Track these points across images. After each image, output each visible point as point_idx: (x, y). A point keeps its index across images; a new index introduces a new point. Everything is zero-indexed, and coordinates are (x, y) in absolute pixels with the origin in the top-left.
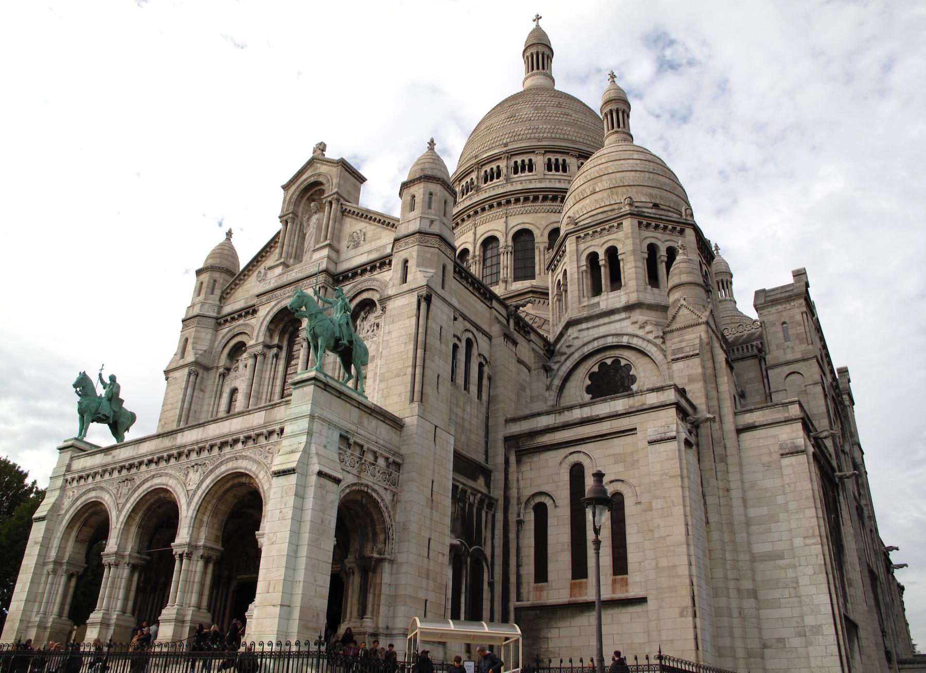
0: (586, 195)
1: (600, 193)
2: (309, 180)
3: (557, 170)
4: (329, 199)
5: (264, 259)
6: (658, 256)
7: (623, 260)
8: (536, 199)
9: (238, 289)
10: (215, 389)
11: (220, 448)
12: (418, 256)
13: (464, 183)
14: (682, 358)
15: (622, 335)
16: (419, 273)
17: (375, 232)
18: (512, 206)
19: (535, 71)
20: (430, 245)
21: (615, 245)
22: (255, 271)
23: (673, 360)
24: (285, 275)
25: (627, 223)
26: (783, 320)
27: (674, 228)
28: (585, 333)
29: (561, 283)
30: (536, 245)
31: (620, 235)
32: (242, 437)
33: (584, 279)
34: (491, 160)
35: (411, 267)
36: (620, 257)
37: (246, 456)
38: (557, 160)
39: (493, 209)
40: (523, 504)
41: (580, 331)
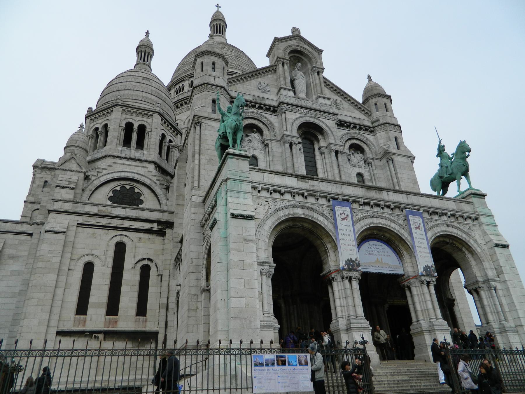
2: (296, 47)
9: (238, 84)
11: (431, 214)
19: (221, 34)
32: (449, 213)
37: (456, 227)
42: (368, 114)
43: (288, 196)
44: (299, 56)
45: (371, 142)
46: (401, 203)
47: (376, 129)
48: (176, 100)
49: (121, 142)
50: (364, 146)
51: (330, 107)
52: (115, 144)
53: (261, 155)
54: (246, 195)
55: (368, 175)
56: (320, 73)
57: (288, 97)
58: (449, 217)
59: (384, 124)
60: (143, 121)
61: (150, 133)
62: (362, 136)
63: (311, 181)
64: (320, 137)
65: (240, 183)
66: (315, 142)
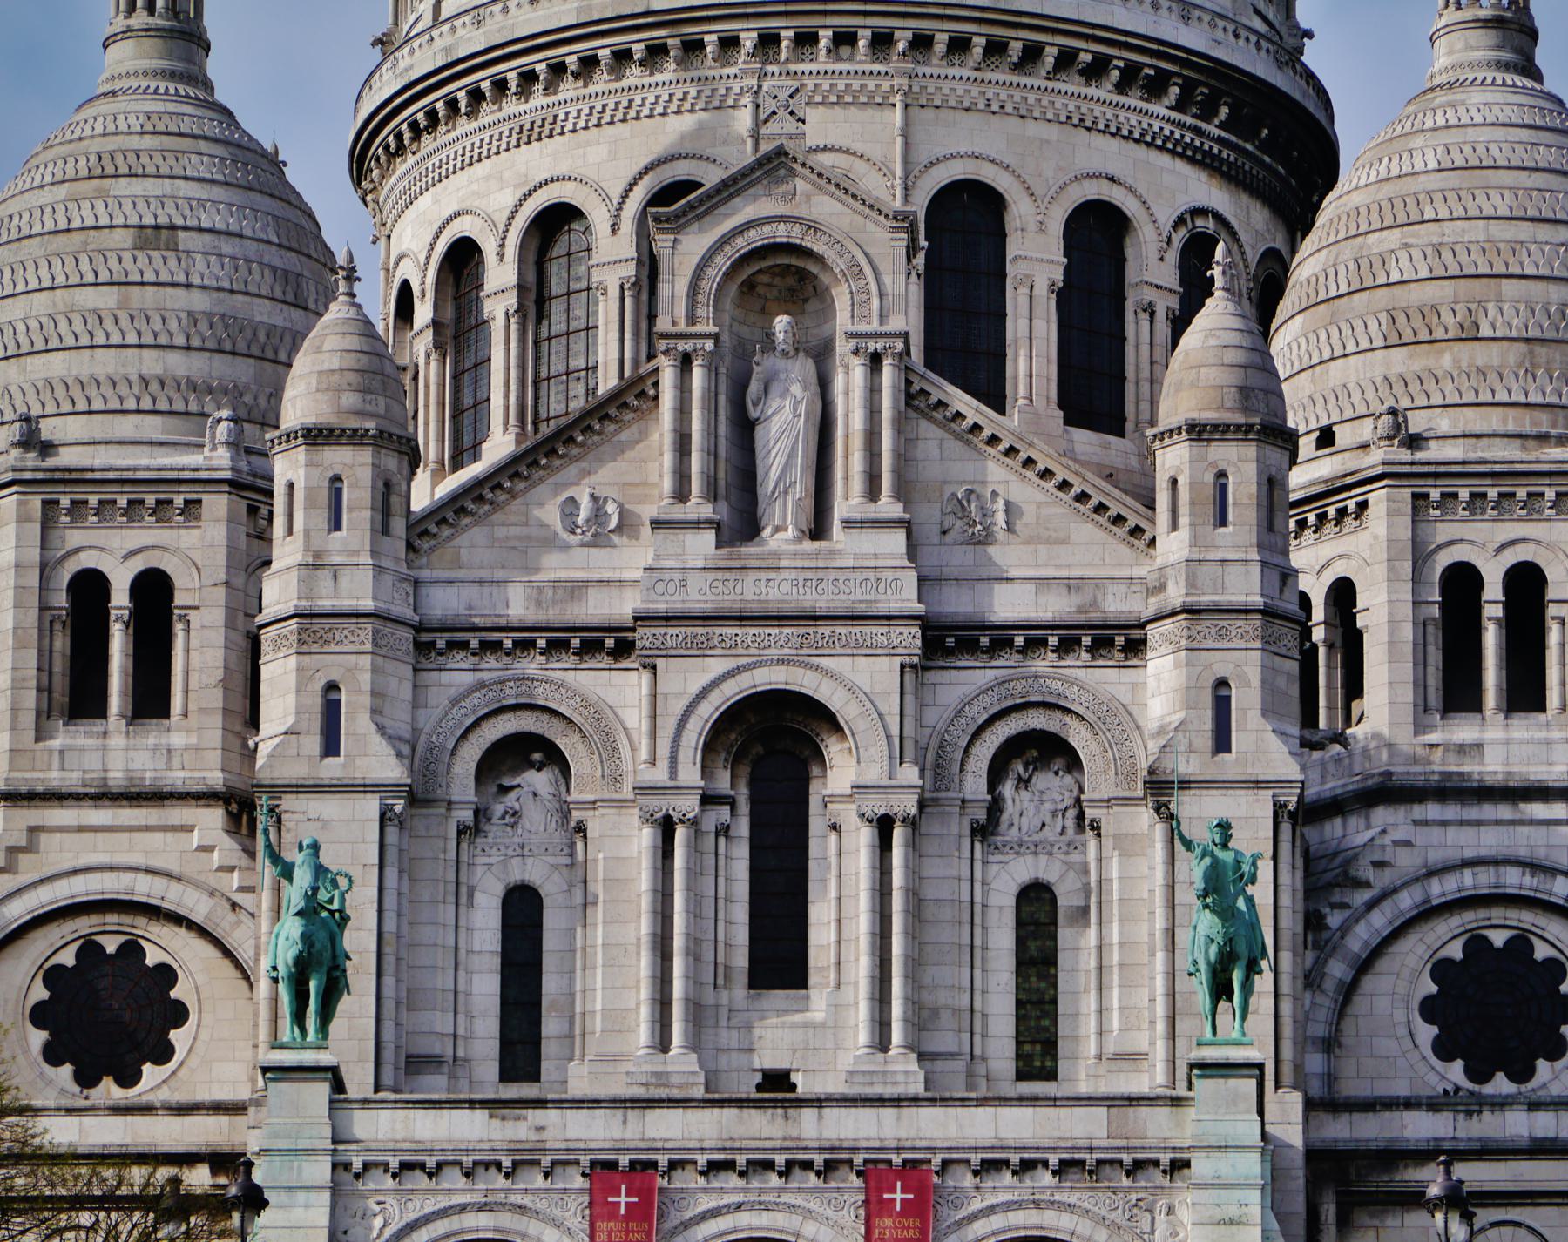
0: (1439, 334)
1: (1495, 346)
2: (767, 229)
4: (872, 346)
5: (575, 451)
8: (1032, 54)
10: (452, 876)
12: (1263, 681)
16: (1273, 737)
17: (1045, 511)
18: (936, 66)
20: (1283, 651)
21: (1542, 564)
22: (534, 485)
24: (752, 576)
28: (1436, 832)
29: (1318, 614)
32: (1053, 1160)
33: (1431, 649)
35: (1244, 711)
36: (1552, 610)
39: (845, 51)
41: (1416, 823)
43: (453, 1179)
44: (794, 261)
46: (855, 1149)
47: (1153, 631)
48: (440, 63)
49: (56, 695)
50: (1078, 737)
51: (889, 575)
52: (28, 719)
53: (556, 876)
54: (313, 1196)
55: (1079, 885)
57: (677, 576)
59: (1174, 614)
60: (154, 548)
61: (193, 616)
63: (539, 1113)
65: (296, 1161)
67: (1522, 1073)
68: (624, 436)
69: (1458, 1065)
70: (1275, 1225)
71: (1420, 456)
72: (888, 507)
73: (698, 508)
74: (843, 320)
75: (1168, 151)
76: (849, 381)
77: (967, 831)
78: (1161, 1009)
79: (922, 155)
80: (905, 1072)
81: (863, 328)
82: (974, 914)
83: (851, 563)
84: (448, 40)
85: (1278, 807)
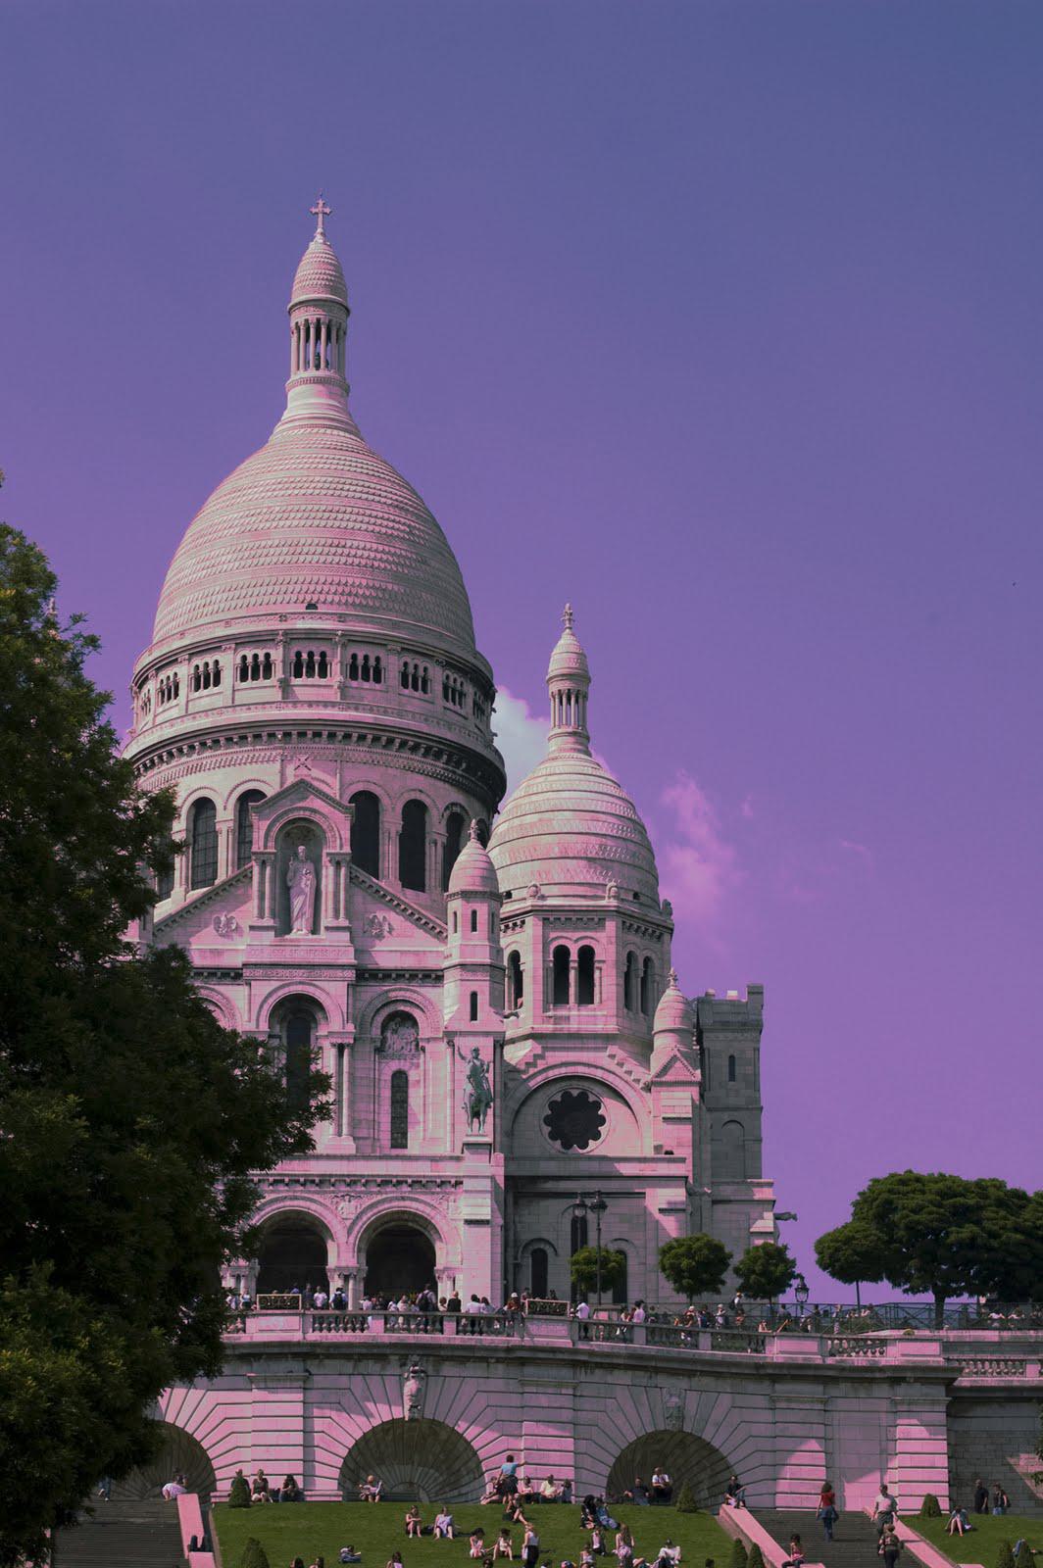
1: (575, 861)
3: (416, 689)
6: (633, 967)
7: (600, 969)
8: (390, 741)
13: (249, 653)
14: (674, 1118)
15: (596, 1067)
23: (664, 1118)
25: (611, 926)
26: (731, 1052)
27: (654, 932)
30: (386, 825)
31: (601, 936)
32: (410, 1181)
34: (311, 635)
36: (597, 965)
38: (416, 667)
39: (317, 739)
40: (521, 1249)
42: (440, 935)
45: (431, 1003)
46: (331, 1176)
47: (447, 974)
50: (417, 1013)
56: (342, 864)
57: (260, 948)
58: (410, 1186)
62: (415, 992)
64: (319, 1015)
66: (313, 1025)
67: (584, 1146)
68: (239, 892)
69: (559, 1142)
70: (496, 1207)
71: (545, 903)
72: (343, 922)
73: (268, 921)
74: (325, 851)
75: (444, 781)
76: (328, 872)
77: (372, 1050)
78: (449, 1121)
79: (347, 780)
80: (348, 1145)
81: (333, 851)
82: (375, 1083)
83: (327, 944)
84: (159, 733)
85: (495, 1042)
